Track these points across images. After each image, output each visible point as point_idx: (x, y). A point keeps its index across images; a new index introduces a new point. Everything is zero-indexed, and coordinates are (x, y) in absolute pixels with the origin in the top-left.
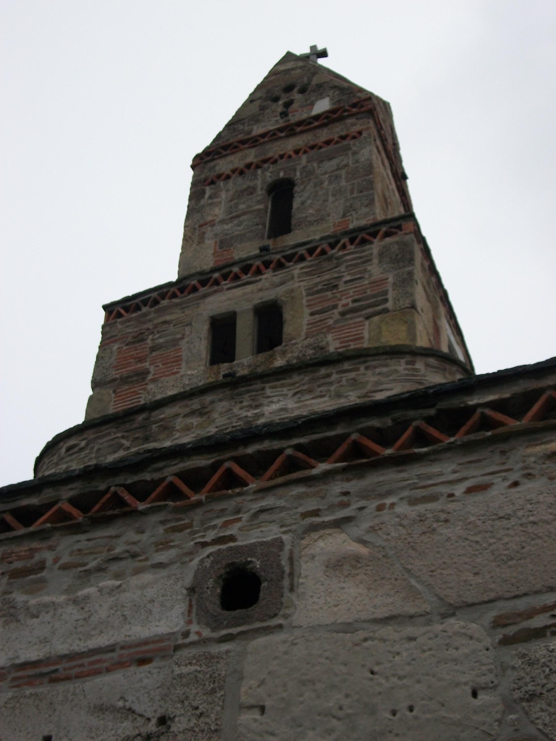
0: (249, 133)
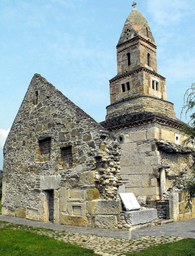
0: (123, 41)
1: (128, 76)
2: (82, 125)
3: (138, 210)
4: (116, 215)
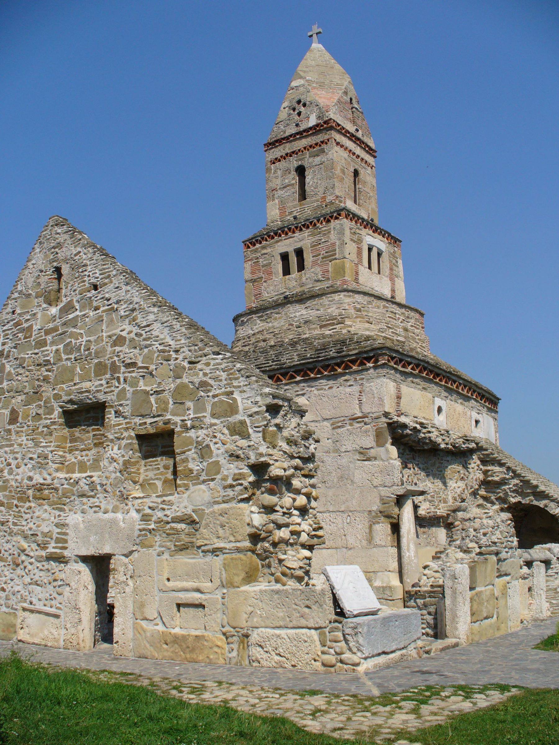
0: (285, 132)
1: (301, 230)
2: (208, 371)
3: (374, 613)
4: (316, 629)
